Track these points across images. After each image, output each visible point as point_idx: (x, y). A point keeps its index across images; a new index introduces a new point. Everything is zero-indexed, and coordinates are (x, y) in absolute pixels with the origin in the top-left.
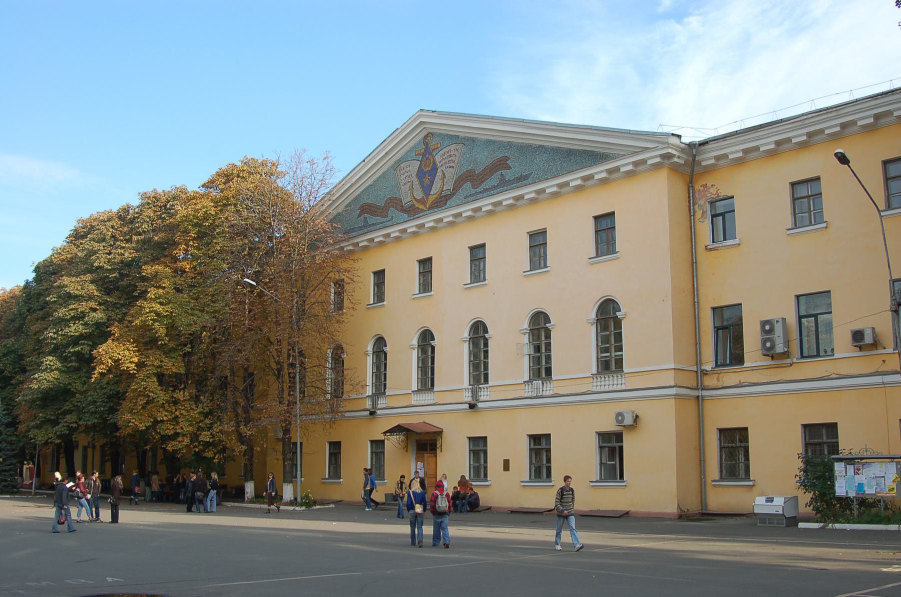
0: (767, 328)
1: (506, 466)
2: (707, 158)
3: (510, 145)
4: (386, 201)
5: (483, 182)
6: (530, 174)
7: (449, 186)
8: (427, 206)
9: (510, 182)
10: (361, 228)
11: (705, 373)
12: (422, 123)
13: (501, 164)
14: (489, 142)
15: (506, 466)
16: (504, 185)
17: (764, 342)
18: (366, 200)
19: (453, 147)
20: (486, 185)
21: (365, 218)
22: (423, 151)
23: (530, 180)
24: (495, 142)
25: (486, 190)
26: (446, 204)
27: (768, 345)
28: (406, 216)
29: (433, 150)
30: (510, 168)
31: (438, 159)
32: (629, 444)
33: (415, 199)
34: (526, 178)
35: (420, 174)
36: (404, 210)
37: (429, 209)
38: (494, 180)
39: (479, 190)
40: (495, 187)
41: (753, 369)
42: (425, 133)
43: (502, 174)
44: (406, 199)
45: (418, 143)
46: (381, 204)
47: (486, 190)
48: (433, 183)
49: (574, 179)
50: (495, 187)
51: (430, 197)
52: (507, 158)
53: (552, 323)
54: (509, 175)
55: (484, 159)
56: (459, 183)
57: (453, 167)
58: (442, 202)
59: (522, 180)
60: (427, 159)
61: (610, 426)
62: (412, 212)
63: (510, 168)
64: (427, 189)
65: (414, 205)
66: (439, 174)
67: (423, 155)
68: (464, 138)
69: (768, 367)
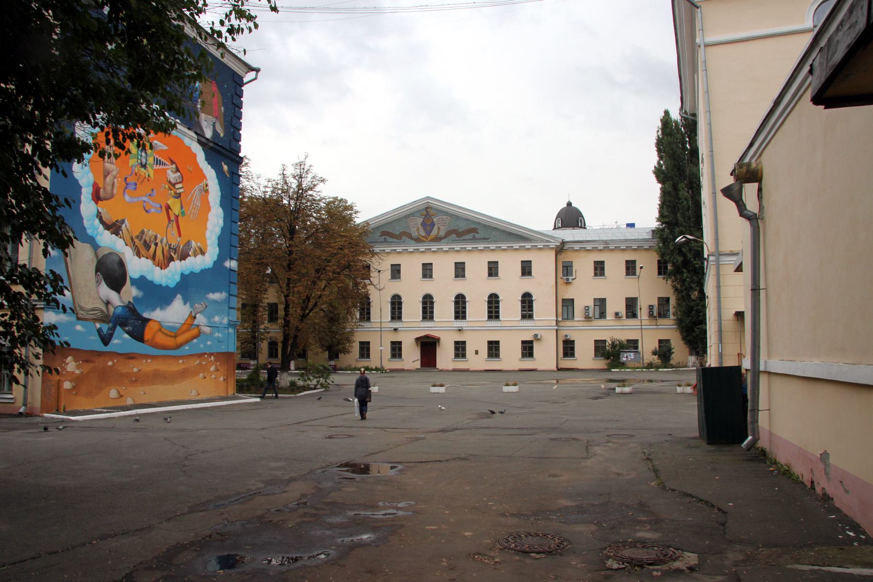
0: (587, 308)
1: (477, 352)
2: (566, 247)
3: (479, 223)
4: (401, 232)
5: (463, 236)
6: (490, 238)
7: (442, 233)
8: (429, 240)
9: (478, 239)
10: (381, 242)
11: (560, 322)
12: (428, 202)
13: (474, 230)
14: (466, 220)
15: (477, 352)
16: (475, 240)
17: (585, 313)
18: (385, 229)
19: (445, 217)
20: (464, 238)
21: (385, 238)
22: (425, 214)
23: (489, 241)
24: (470, 220)
25: (464, 240)
26: (440, 241)
27: (587, 314)
28: (414, 242)
29: (432, 215)
30: (478, 233)
31: (435, 220)
32: (536, 346)
33: (421, 235)
34: (487, 239)
35: (423, 224)
36: (412, 238)
37: (429, 241)
38: (470, 236)
39: (460, 239)
40: (469, 239)
41: (578, 321)
42: (427, 206)
43: (474, 235)
44: (415, 234)
45: (422, 210)
46: (398, 233)
47: (464, 240)
48: (432, 230)
49: (516, 246)
50: (469, 239)
51: (430, 236)
52: (477, 229)
53: (500, 298)
54: (477, 236)
55: (463, 227)
56: (448, 234)
57: (445, 226)
58: (437, 239)
59: (485, 239)
60: (428, 218)
61: (529, 337)
62: (418, 240)
63: (478, 233)
64: (429, 233)
65: (419, 238)
66: (436, 227)
67: (425, 216)
68: (451, 214)
69: (583, 321)
